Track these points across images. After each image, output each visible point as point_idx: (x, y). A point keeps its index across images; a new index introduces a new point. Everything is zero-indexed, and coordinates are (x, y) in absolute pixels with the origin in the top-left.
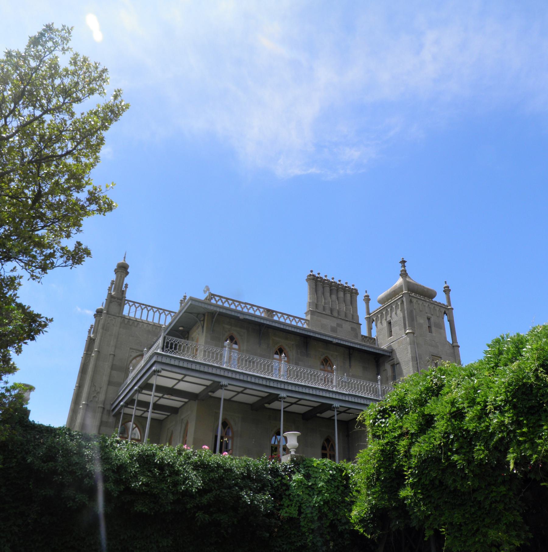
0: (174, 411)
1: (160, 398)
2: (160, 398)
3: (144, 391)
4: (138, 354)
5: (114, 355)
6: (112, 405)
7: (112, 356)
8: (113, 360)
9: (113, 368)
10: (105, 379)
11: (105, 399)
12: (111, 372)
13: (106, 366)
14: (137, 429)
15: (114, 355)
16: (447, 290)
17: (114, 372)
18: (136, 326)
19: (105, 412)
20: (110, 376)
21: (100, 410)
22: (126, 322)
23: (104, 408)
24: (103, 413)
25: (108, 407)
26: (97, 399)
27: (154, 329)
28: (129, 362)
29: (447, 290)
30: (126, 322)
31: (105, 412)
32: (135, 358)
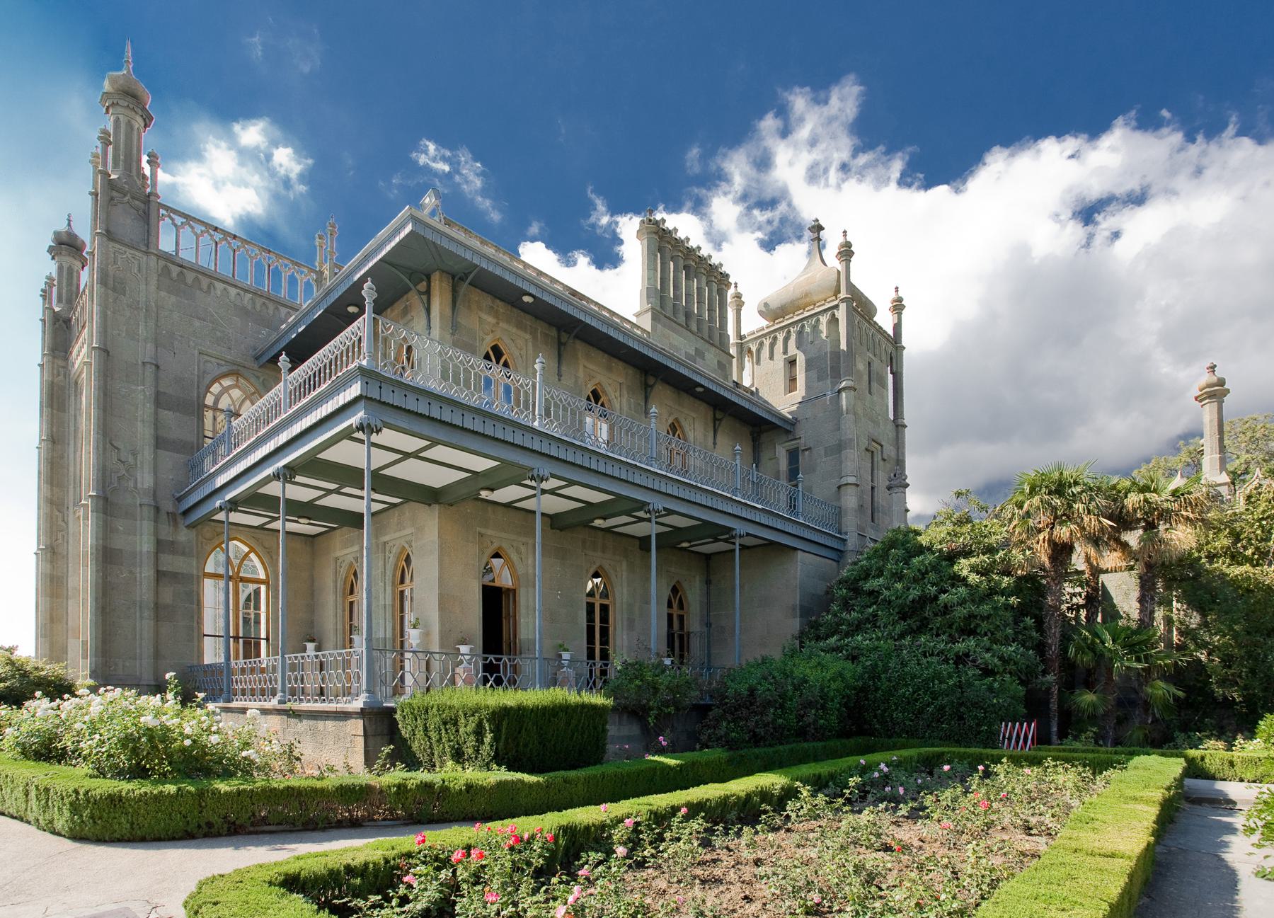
0: (354, 520)
1: (329, 492)
2: (329, 492)
3: (298, 479)
4: (224, 369)
5: (157, 367)
6: (180, 499)
7: (150, 370)
8: (157, 378)
9: (160, 401)
10: (144, 433)
11: (156, 484)
12: (156, 413)
13: (140, 397)
14: (252, 556)
15: (157, 367)
16: (898, 307)
17: (167, 415)
18: (208, 292)
19: (164, 517)
20: (157, 424)
21: (148, 512)
22: (174, 275)
23: (157, 509)
24: (156, 521)
25: (168, 506)
26: (131, 484)
27: (258, 307)
28: (203, 389)
29: (898, 307)
30: (174, 275)
31: (164, 517)
32: (216, 379)
